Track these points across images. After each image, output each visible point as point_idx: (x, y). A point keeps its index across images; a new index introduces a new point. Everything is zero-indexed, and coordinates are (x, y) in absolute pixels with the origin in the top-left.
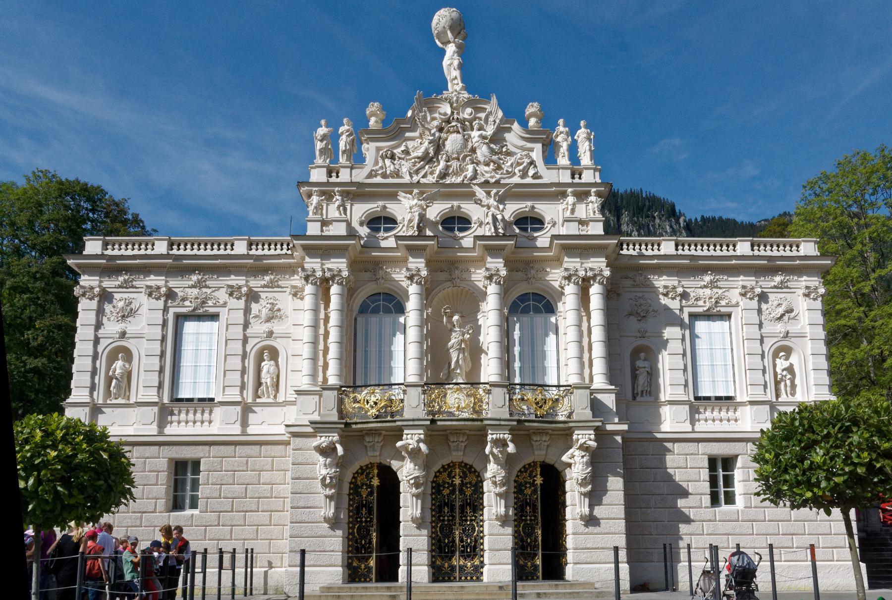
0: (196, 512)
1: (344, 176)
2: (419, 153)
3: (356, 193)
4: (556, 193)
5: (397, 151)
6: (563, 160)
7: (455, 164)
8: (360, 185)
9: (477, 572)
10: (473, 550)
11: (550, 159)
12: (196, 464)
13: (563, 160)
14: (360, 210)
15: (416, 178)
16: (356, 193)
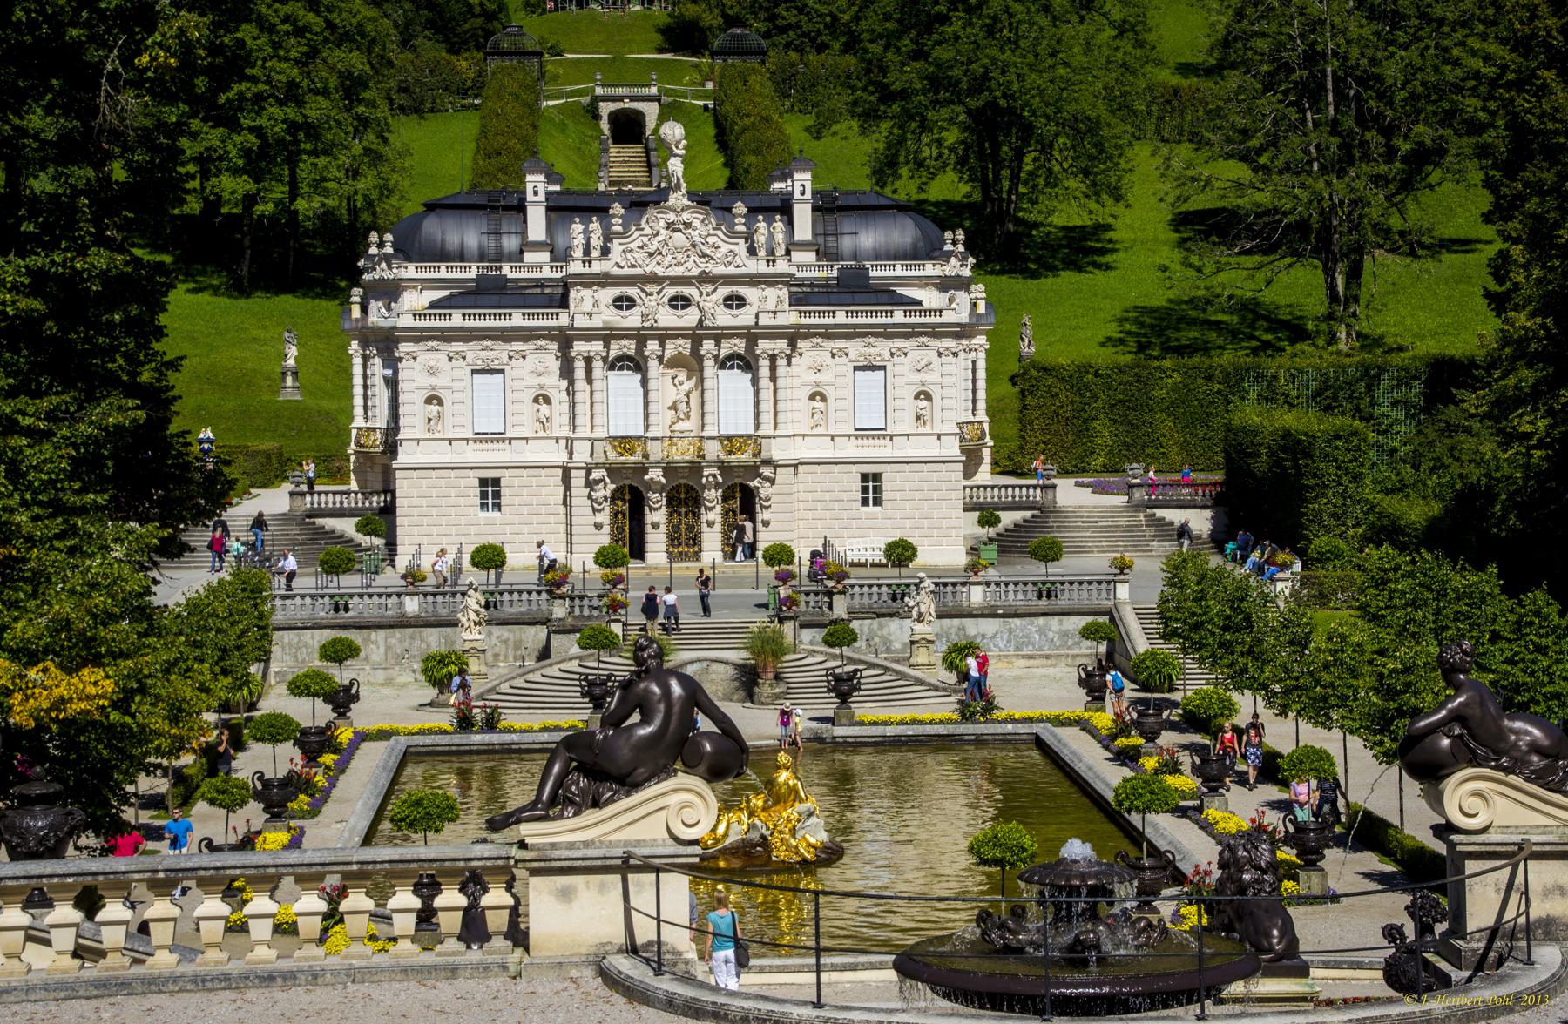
0: (496, 514)
1: (597, 268)
2: (652, 249)
3: (605, 280)
4: (754, 280)
5: (633, 246)
6: (762, 253)
7: (679, 256)
8: (606, 275)
9: (697, 556)
10: (695, 540)
11: (752, 251)
12: (496, 482)
13: (762, 253)
14: (608, 294)
15: (648, 270)
16: (605, 280)
